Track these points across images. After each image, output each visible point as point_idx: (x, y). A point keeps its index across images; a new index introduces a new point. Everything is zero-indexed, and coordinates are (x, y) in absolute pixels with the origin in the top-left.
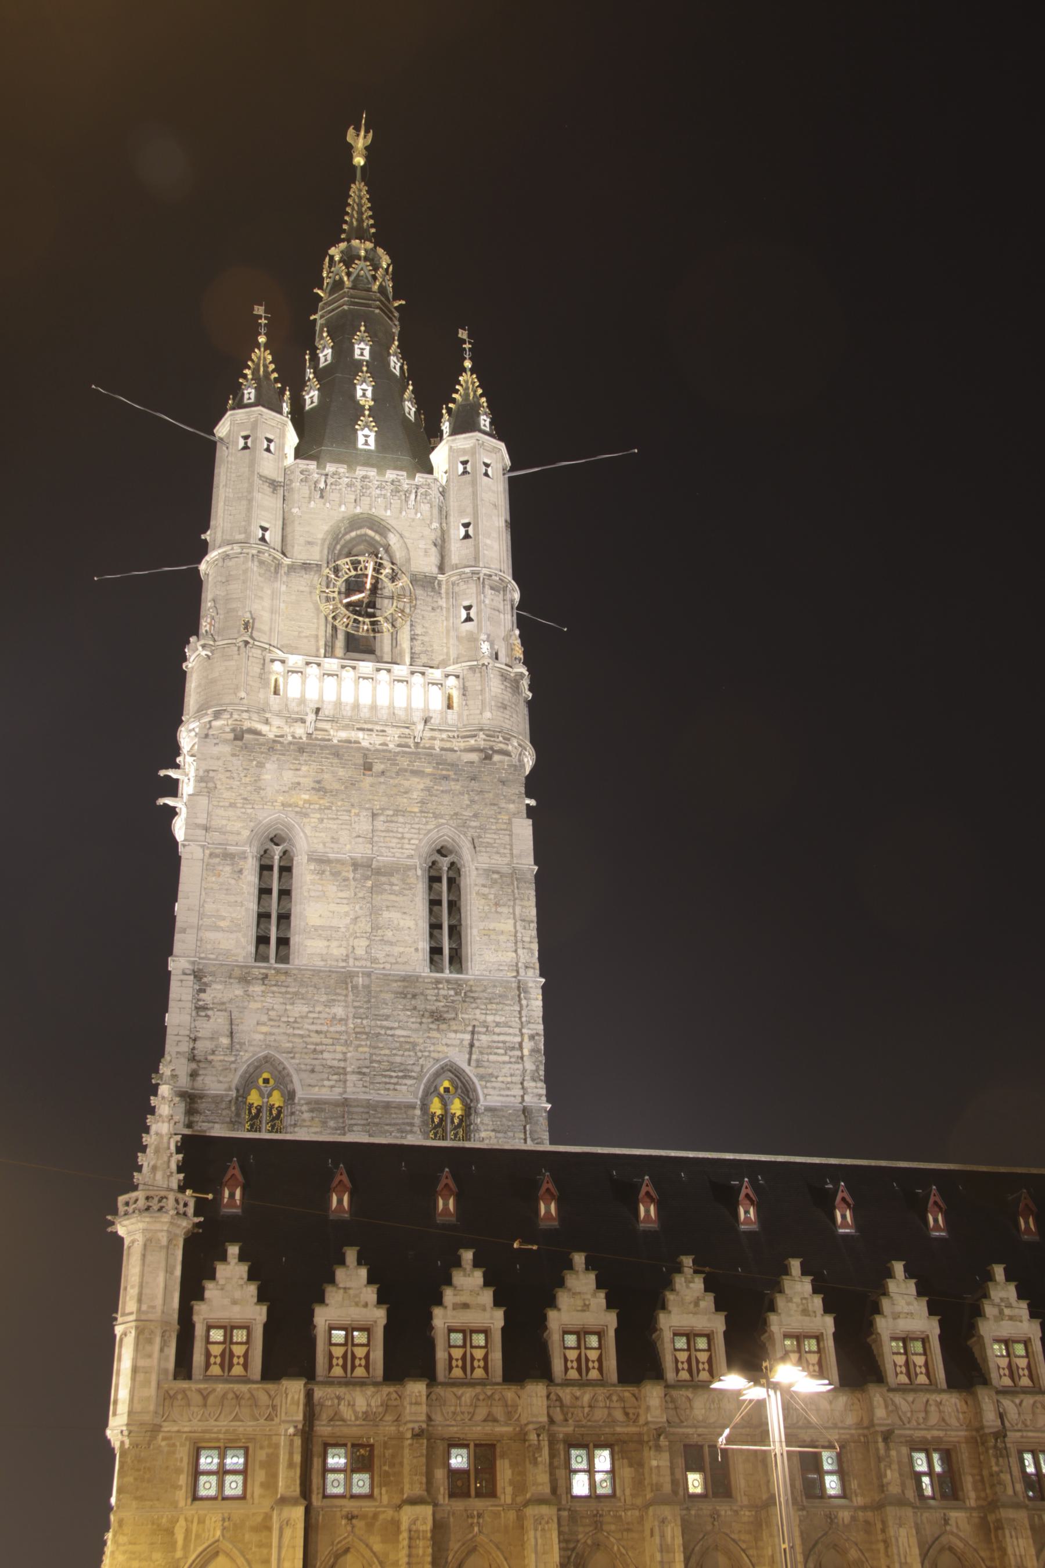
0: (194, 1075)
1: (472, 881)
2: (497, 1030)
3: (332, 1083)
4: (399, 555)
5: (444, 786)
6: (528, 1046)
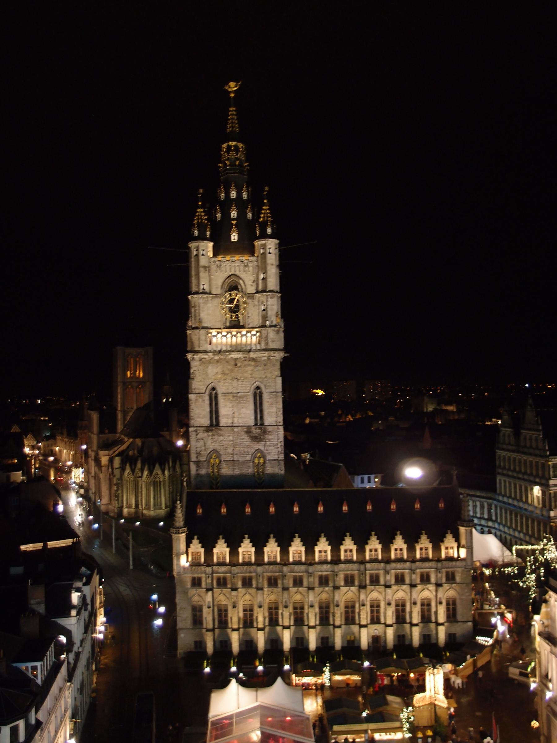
0: (197, 457)
1: (266, 396)
3: (230, 457)
4: (244, 287)
6: (279, 444)
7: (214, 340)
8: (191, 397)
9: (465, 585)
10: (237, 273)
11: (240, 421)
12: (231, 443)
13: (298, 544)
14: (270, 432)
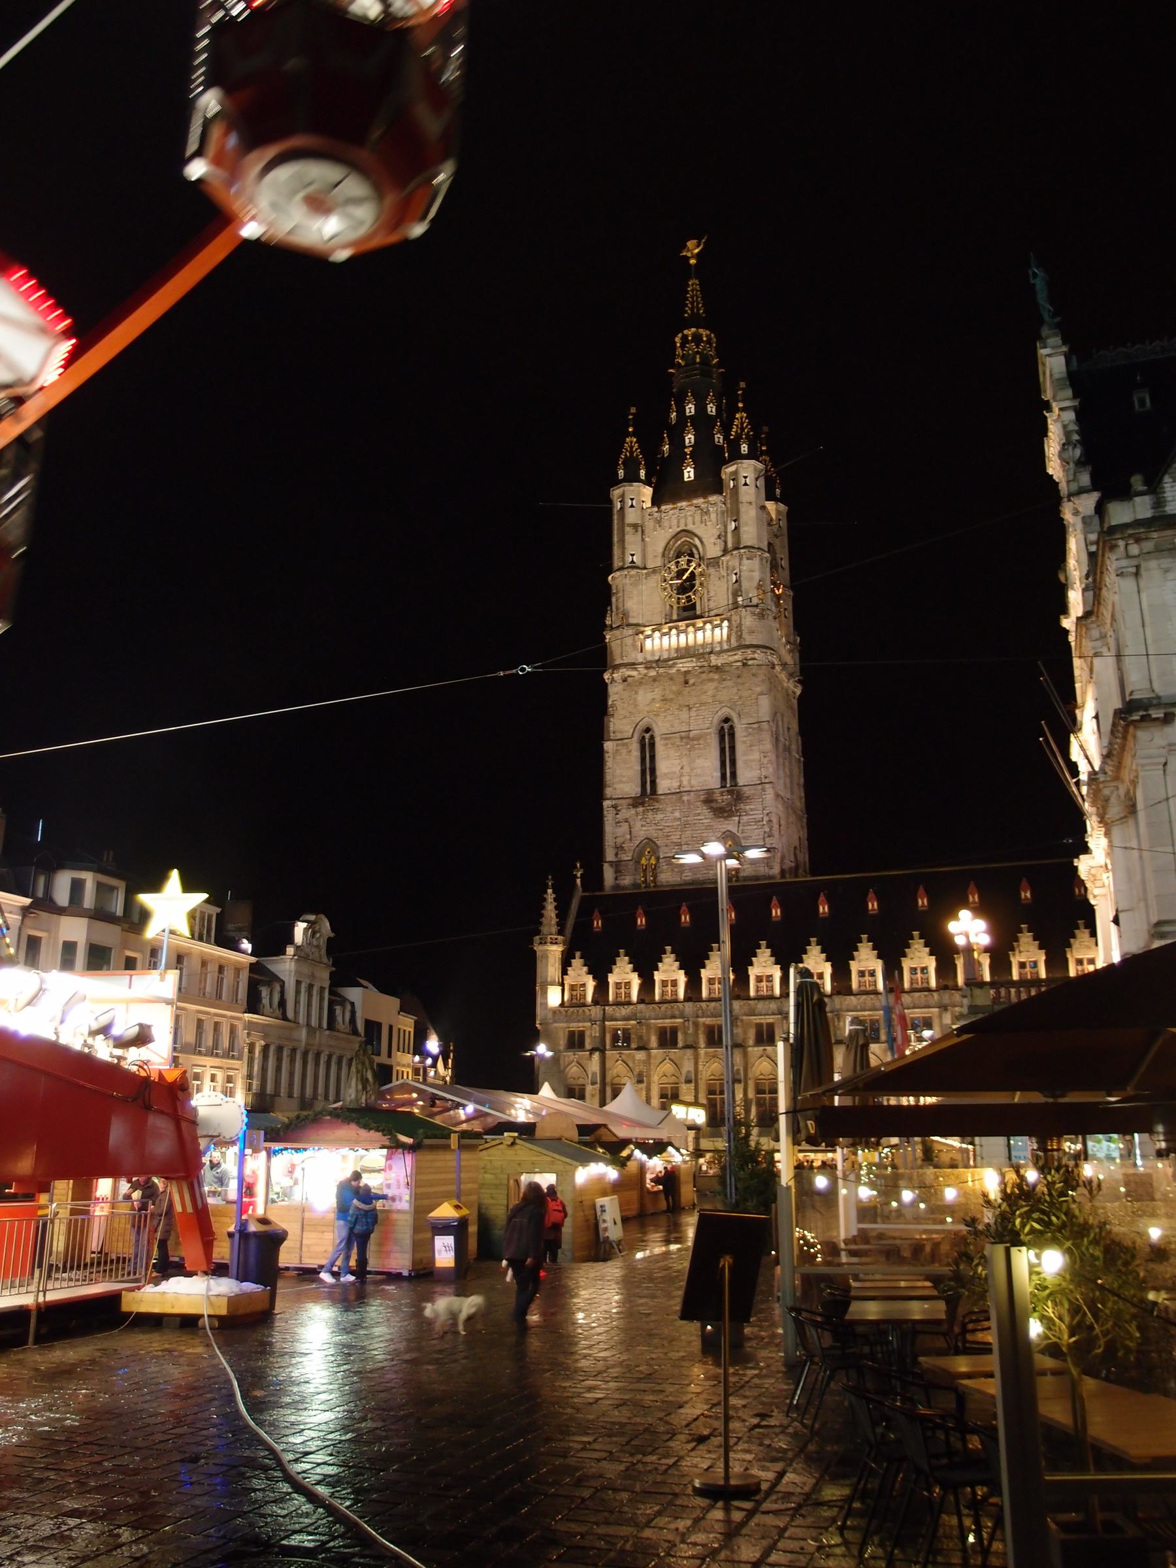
0: (616, 855)
4: (701, 550)
5: (725, 684)
7: (648, 644)
8: (608, 746)
10: (690, 527)
11: (693, 782)
13: (766, 962)
14: (748, 798)
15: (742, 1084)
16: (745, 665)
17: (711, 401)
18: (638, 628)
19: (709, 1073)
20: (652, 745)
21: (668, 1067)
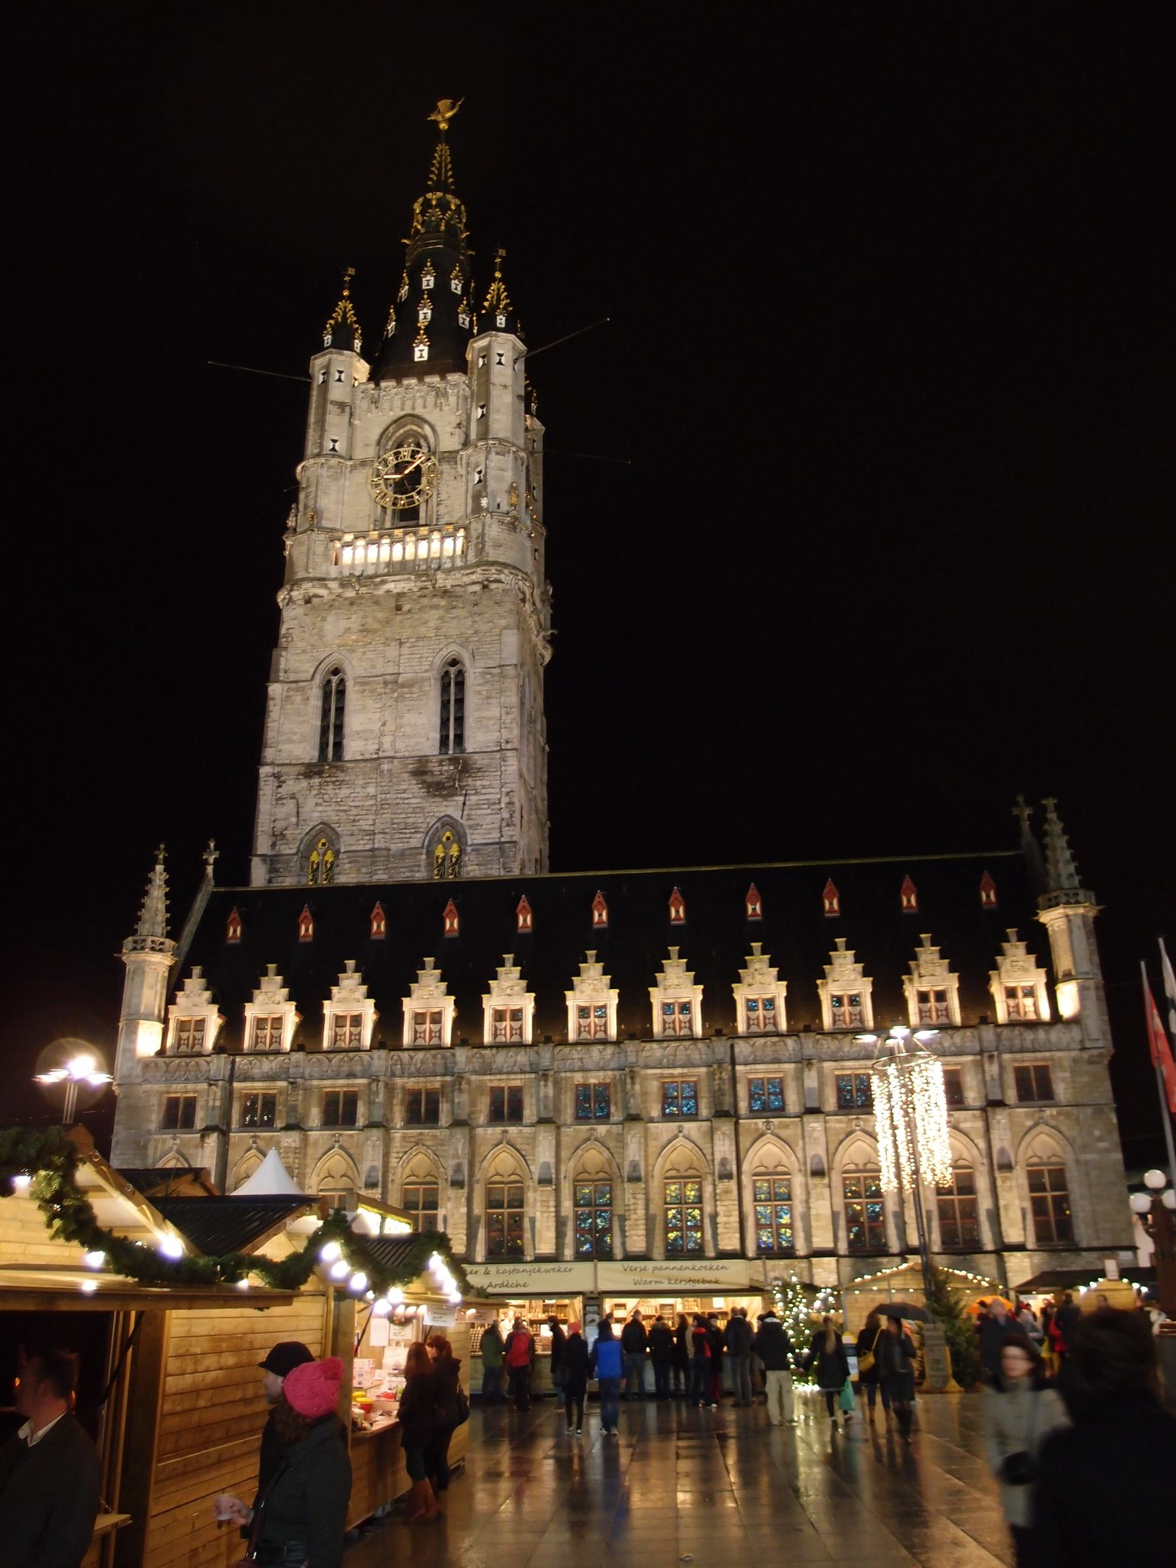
0: (274, 845)
2: (484, 791)
4: (432, 440)
7: (347, 556)
8: (274, 689)
9: (1090, 1110)
10: (419, 411)
11: (400, 745)
12: (372, 802)
13: (512, 987)
14: (479, 770)
15: (466, 1190)
16: (485, 587)
17: (456, 277)
18: (334, 535)
19: (407, 1171)
20: (341, 693)
21: (336, 1161)
